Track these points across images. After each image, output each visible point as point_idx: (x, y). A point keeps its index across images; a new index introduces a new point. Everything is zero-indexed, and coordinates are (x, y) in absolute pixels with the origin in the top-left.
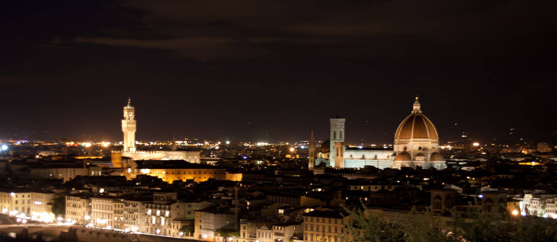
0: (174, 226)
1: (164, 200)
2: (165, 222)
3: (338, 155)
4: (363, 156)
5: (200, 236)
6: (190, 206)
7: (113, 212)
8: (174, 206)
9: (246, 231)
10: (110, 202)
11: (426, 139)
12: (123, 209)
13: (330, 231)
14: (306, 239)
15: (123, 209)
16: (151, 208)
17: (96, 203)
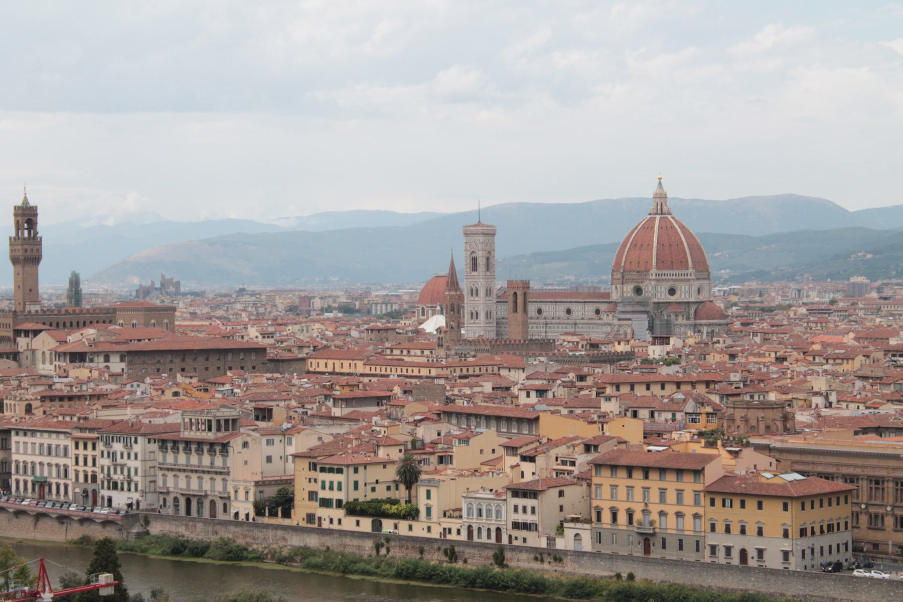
0: (236, 492)
1: (210, 430)
2: (213, 486)
3: (515, 311)
4: (540, 311)
5: (310, 518)
6: (269, 443)
7: (70, 462)
8: (236, 444)
9: (433, 502)
10: (62, 436)
11: (686, 272)
12: (97, 453)
13: (662, 499)
14: (599, 519)
15: (97, 453)
16: (175, 449)
17: (21, 439)
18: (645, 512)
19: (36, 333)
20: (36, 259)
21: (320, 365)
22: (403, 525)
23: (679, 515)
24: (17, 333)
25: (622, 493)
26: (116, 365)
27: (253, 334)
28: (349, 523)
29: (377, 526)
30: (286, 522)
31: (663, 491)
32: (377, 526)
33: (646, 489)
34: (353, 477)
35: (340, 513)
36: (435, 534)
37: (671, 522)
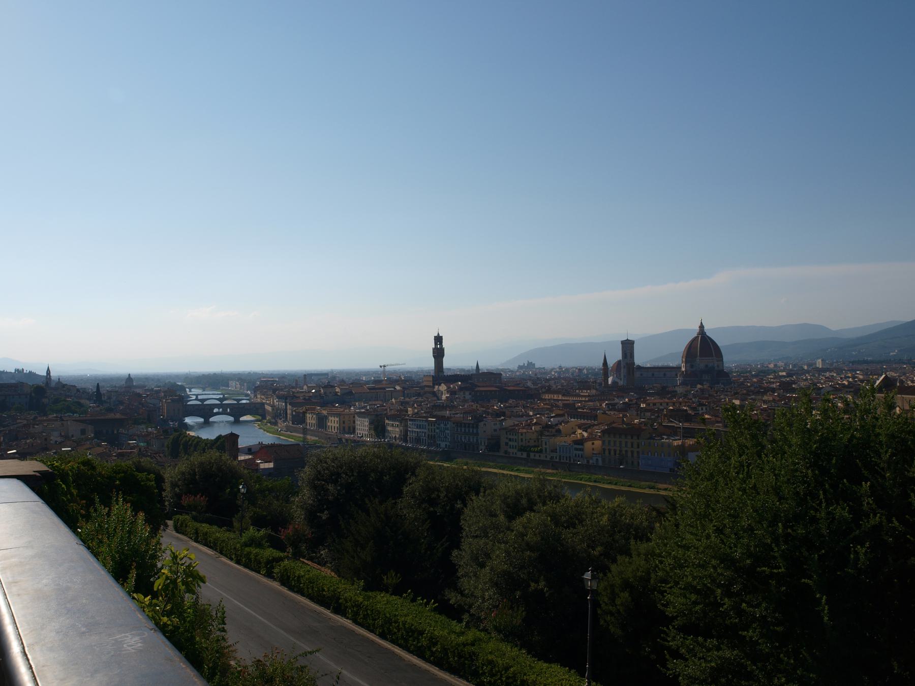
5: (506, 452)
13: (626, 446)
18: (621, 451)
19: (440, 385)
20: (443, 355)
21: (547, 397)
22: (537, 455)
23: (632, 452)
24: (434, 384)
25: (612, 444)
26: (468, 396)
27: (529, 384)
28: (519, 454)
29: (528, 456)
30: (497, 454)
31: (626, 442)
32: (528, 456)
33: (620, 442)
34: (520, 437)
35: (515, 451)
36: (548, 459)
37: (629, 454)
